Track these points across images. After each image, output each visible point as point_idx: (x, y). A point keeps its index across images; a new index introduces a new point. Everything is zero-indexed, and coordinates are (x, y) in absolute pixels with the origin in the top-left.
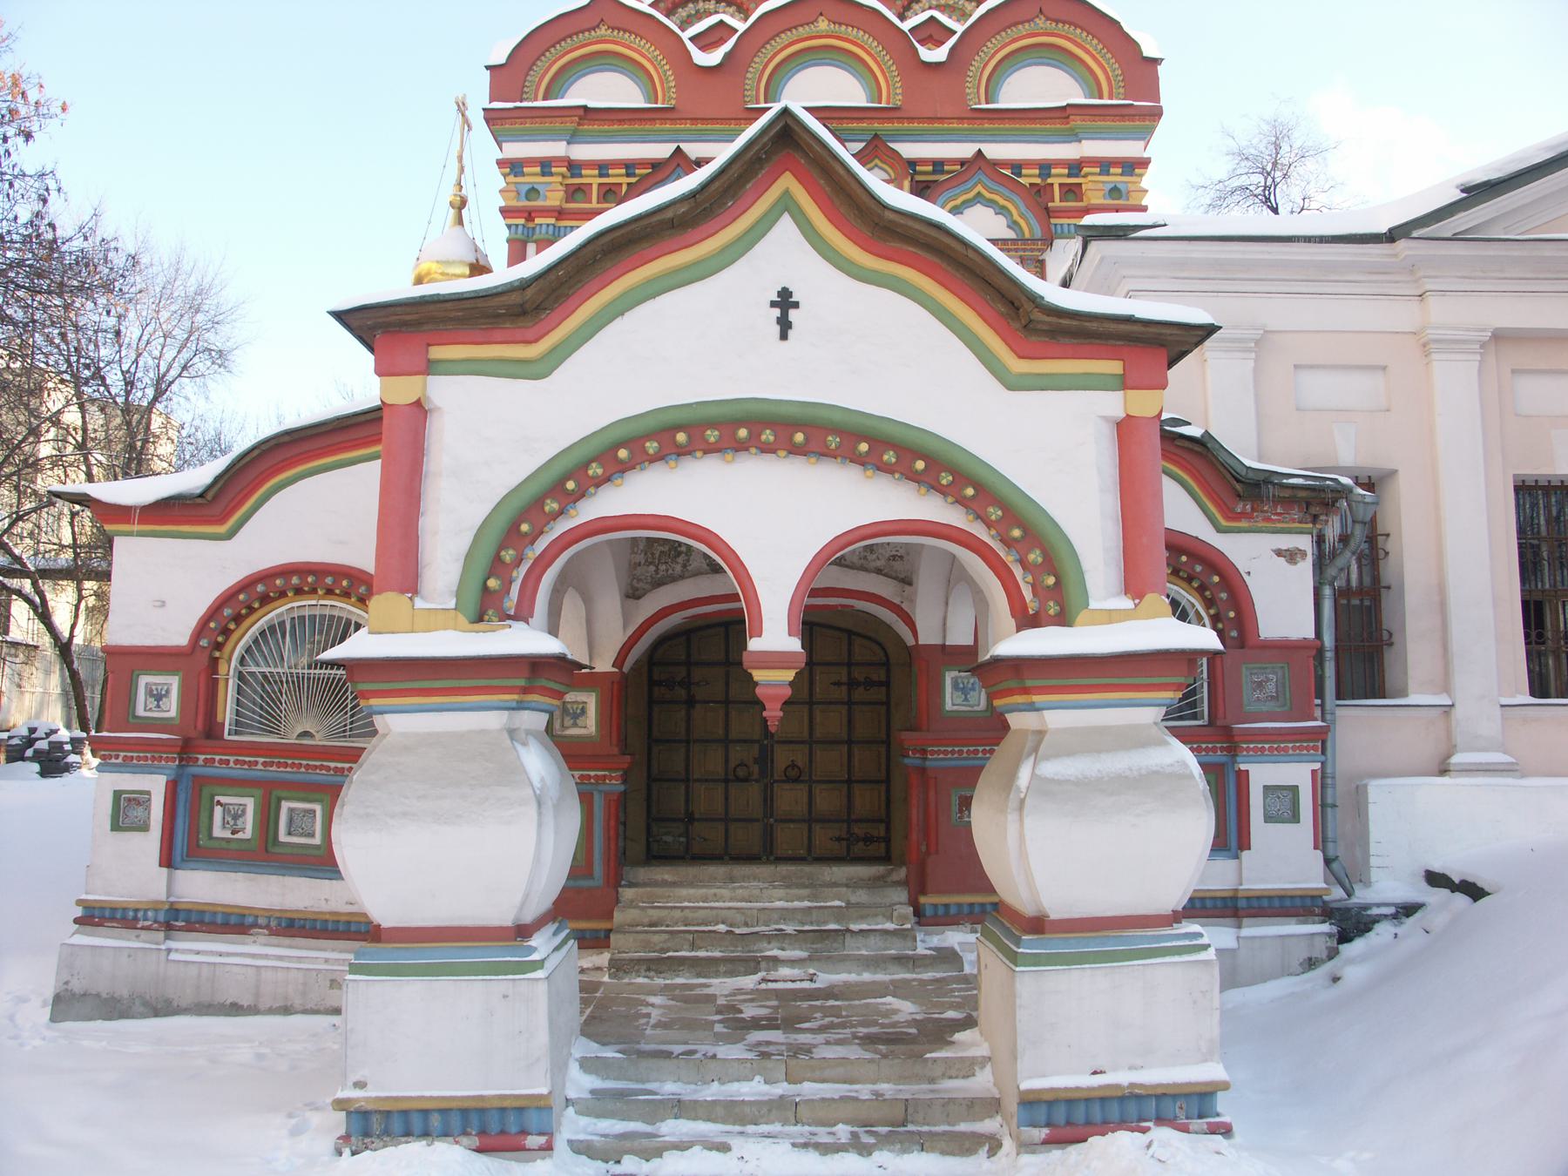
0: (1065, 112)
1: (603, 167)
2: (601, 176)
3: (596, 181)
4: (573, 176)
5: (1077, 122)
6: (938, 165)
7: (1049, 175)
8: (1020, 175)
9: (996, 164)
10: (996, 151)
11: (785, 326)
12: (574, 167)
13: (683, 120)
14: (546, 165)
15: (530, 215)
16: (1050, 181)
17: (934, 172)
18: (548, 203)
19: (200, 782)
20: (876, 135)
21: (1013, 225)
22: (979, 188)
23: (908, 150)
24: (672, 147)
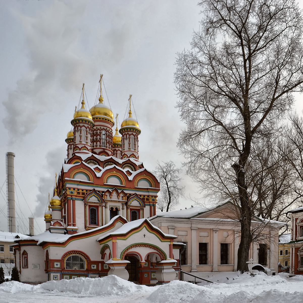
0: (147, 189)
1: (83, 190)
3: (81, 192)
8: (141, 196)
11: (144, 237)
12: (78, 190)
13: (94, 184)
14: (74, 189)
17: (130, 195)
18: (74, 195)
19: (62, 274)
21: (140, 204)
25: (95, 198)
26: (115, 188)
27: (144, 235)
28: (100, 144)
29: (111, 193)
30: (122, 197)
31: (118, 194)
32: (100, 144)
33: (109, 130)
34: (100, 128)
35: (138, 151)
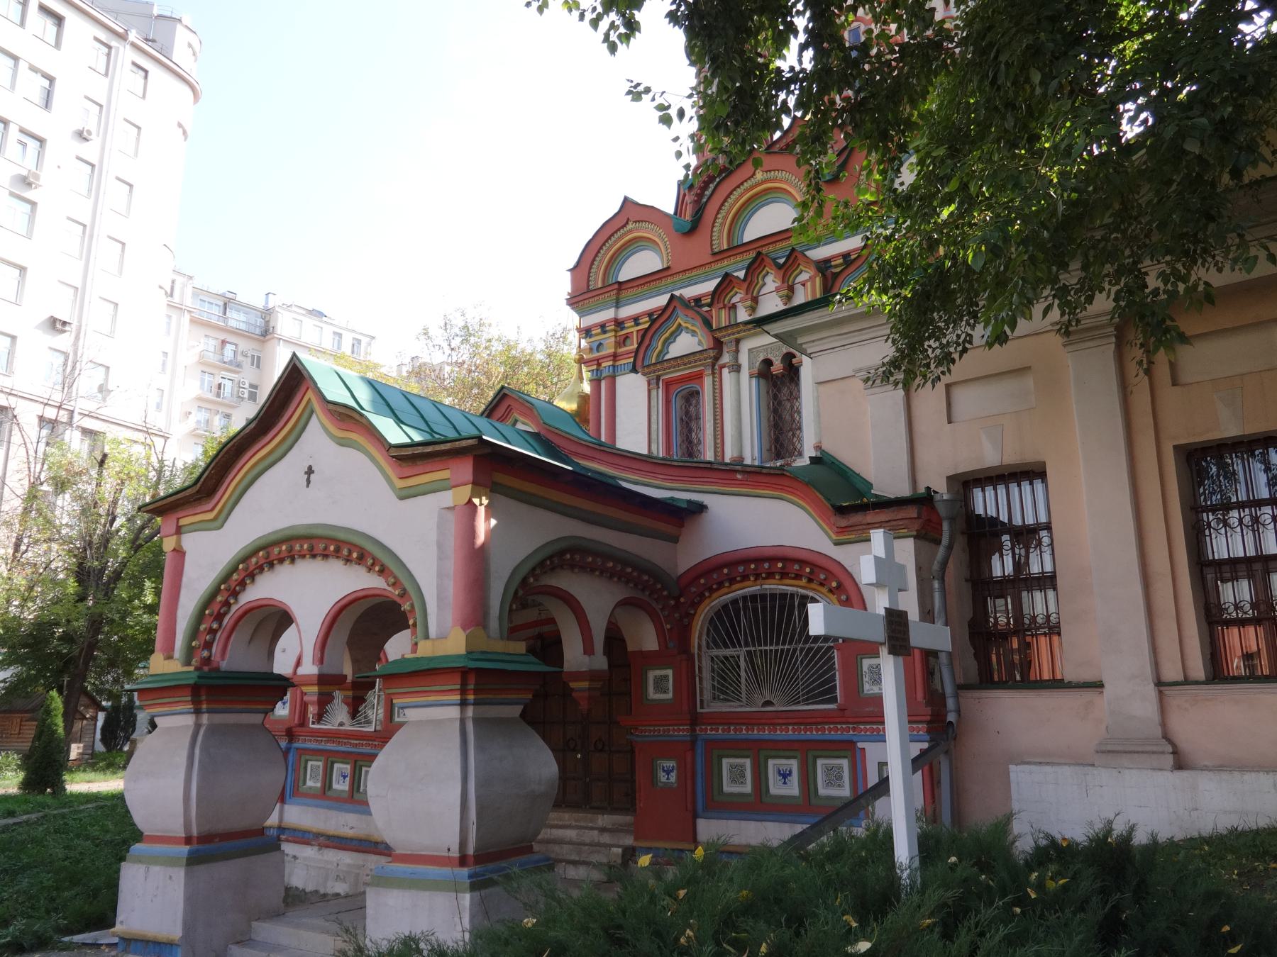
1: (636, 319)
2: (637, 324)
4: (622, 329)
6: (846, 256)
11: (308, 481)
12: (619, 323)
14: (603, 326)
15: (598, 362)
20: (793, 250)
26: (760, 256)
27: (310, 471)
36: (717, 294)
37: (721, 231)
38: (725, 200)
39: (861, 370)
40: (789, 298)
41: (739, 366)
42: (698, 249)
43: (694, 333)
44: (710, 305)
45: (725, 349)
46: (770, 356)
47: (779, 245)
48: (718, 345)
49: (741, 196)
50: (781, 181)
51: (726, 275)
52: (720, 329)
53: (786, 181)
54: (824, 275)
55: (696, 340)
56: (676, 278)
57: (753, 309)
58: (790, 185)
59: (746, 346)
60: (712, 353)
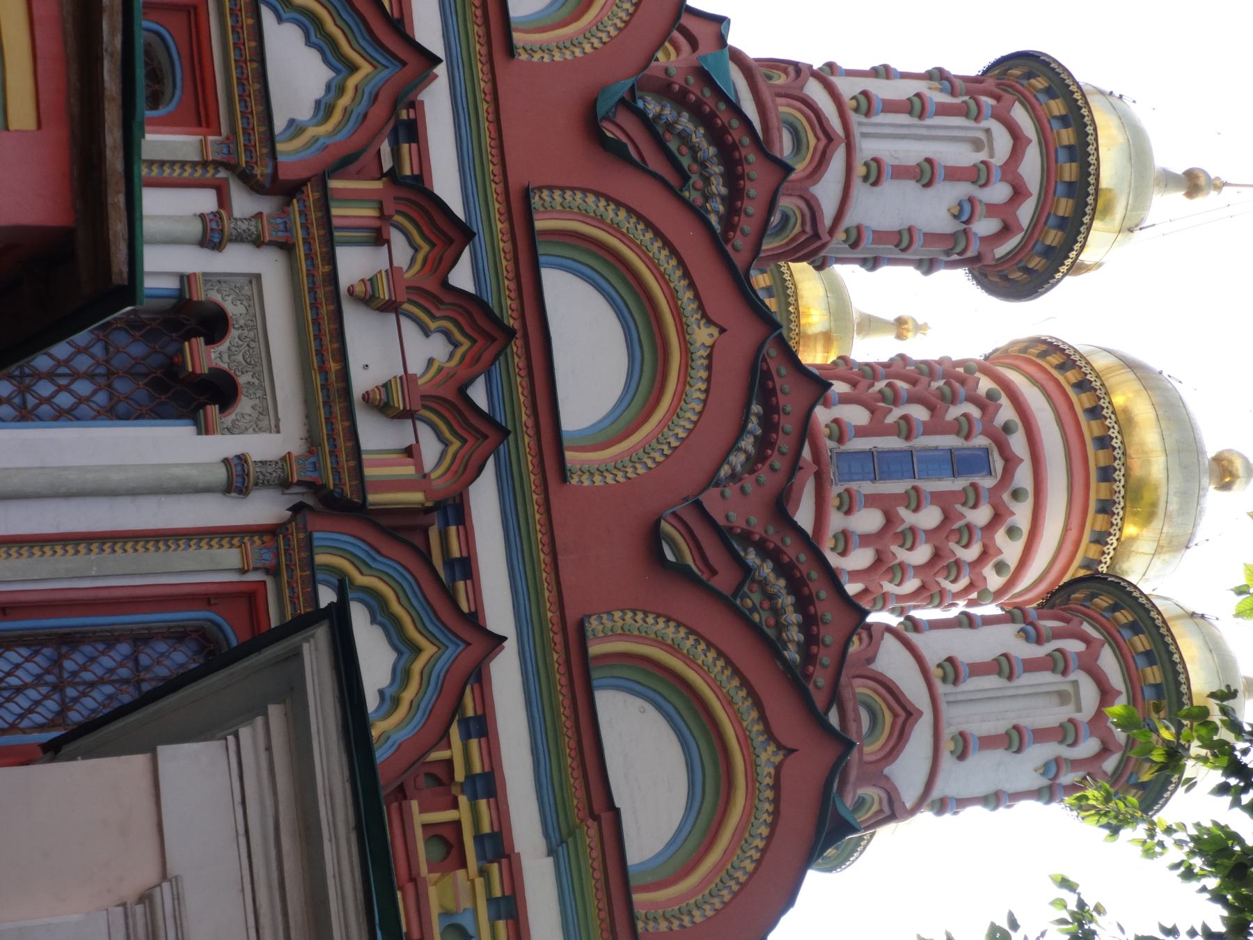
5: (589, 836)
6: (466, 567)
7: (474, 798)
8: (466, 736)
9: (479, 676)
10: (506, 674)
16: (463, 800)
17: (449, 562)
20: (504, 433)
22: (429, 650)
23: (484, 500)
24: (437, 48)
25: (319, 92)
26: (508, 335)
28: (861, 432)
29: (427, 298)
30: (410, 452)
31: (446, 404)
32: (861, 432)
33: (1000, 567)
34: (1007, 428)
35: (941, 806)
36: (414, 191)
37: (584, 215)
38: (658, 234)
39: (178, 898)
40: (382, 405)
41: (217, 246)
42: (543, 138)
43: (324, 109)
44: (393, 176)
45: (266, 205)
46: (233, 333)
47: (520, 382)
48: (285, 190)
49: (662, 277)
50: (681, 395)
51: (465, 233)
52: (324, 204)
53: (675, 411)
54: (427, 511)
55: (305, 113)
56: (480, 69)
57: (368, 299)
58: (666, 423)
59: (268, 267)
60: (262, 171)
